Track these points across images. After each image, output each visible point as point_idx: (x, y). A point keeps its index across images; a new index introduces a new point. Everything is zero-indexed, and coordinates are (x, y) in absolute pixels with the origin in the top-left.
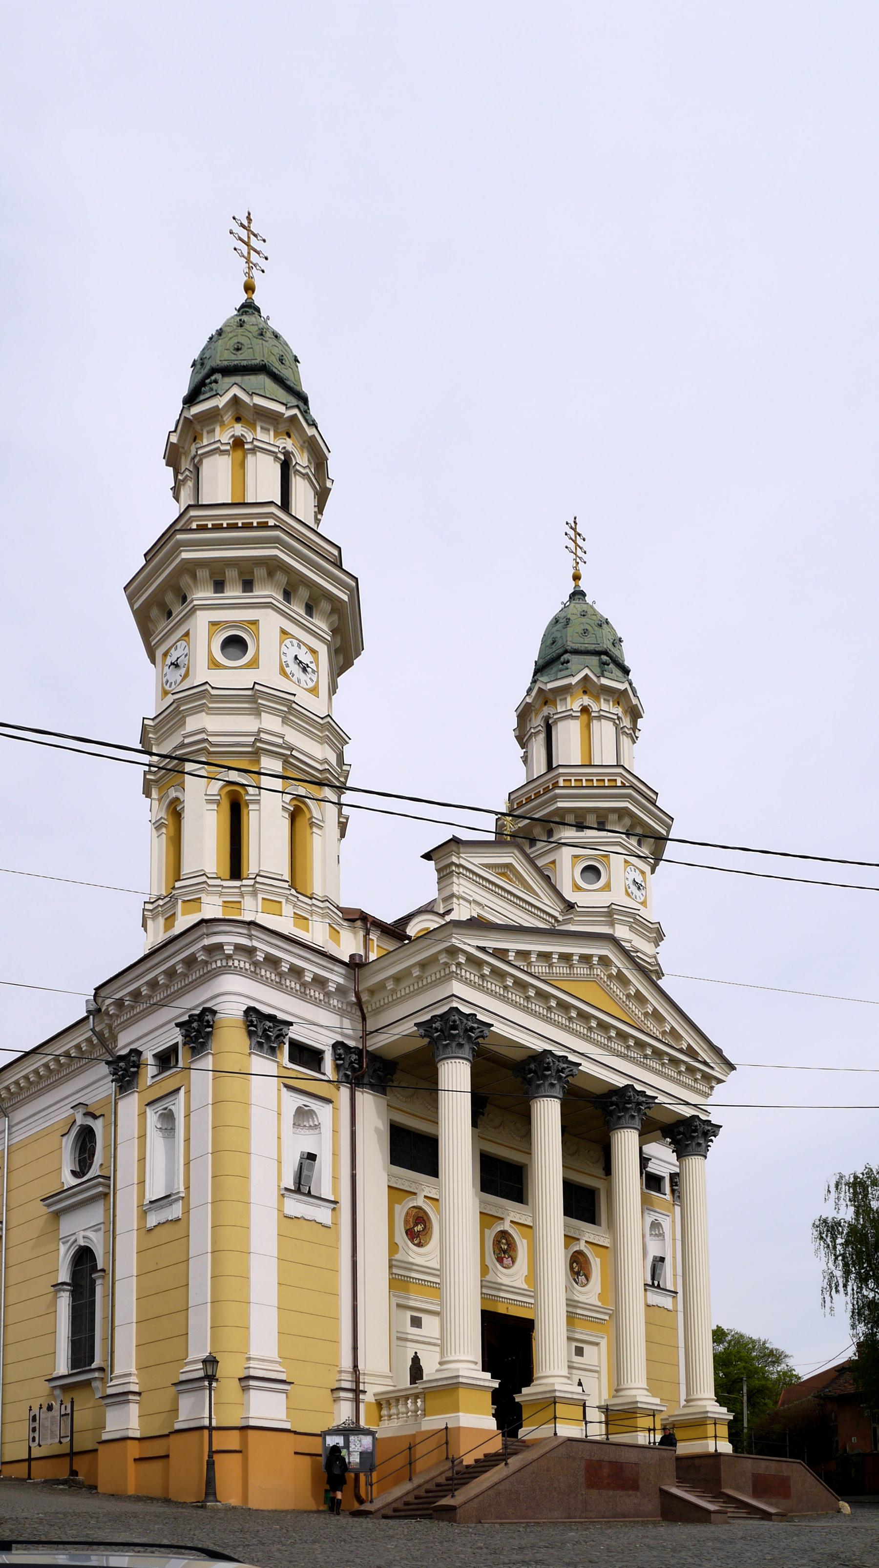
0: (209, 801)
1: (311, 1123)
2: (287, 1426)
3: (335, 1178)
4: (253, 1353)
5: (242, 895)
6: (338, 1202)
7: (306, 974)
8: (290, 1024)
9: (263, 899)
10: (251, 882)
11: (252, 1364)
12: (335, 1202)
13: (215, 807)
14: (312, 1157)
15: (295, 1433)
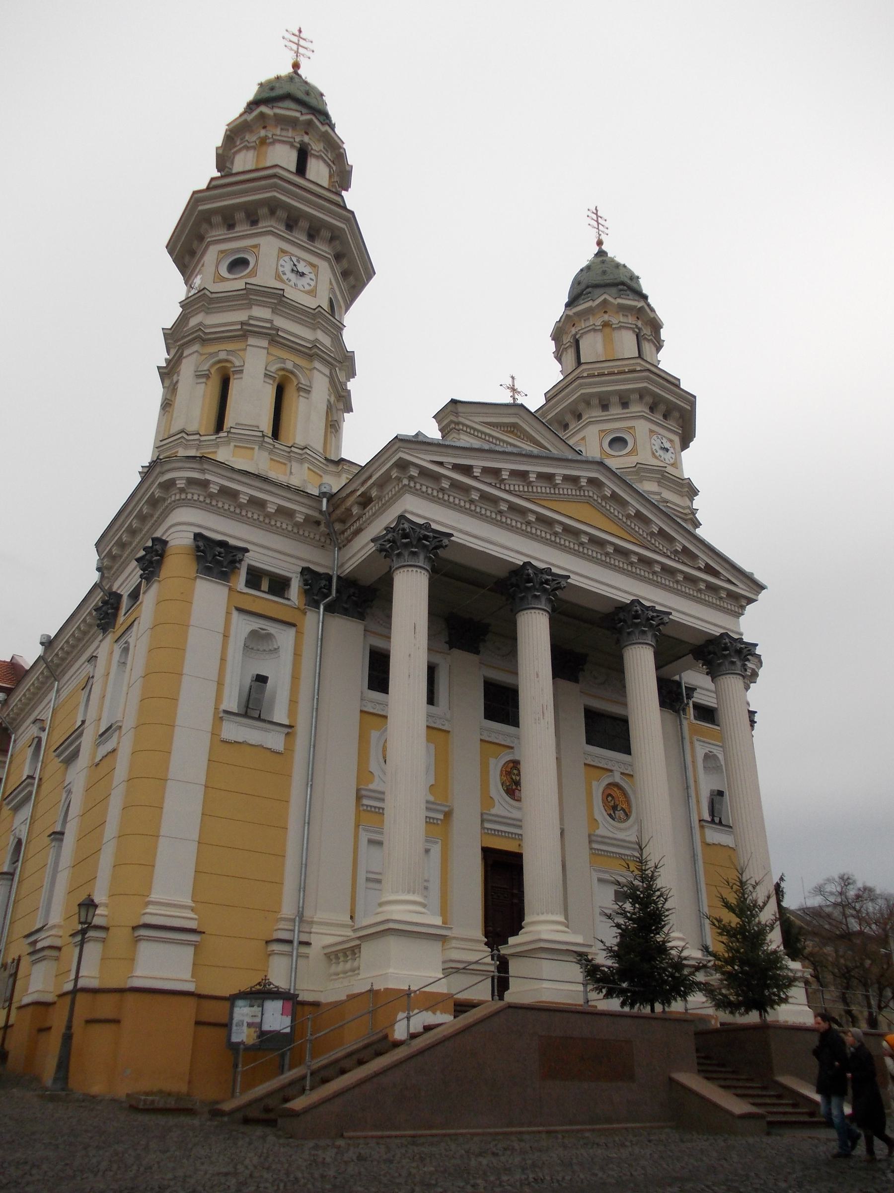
0: (198, 376)
1: (271, 648)
2: (190, 987)
3: (293, 702)
4: (154, 897)
5: (217, 446)
6: (293, 727)
7: (268, 505)
8: (246, 550)
9: (235, 446)
10: (225, 434)
11: (150, 909)
12: (290, 727)
13: (204, 380)
14: (262, 679)
15: (200, 996)
